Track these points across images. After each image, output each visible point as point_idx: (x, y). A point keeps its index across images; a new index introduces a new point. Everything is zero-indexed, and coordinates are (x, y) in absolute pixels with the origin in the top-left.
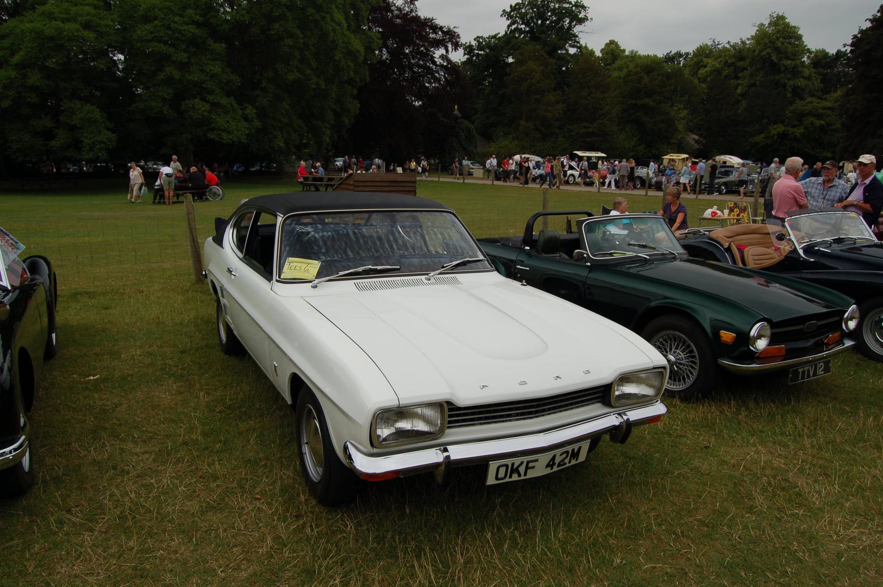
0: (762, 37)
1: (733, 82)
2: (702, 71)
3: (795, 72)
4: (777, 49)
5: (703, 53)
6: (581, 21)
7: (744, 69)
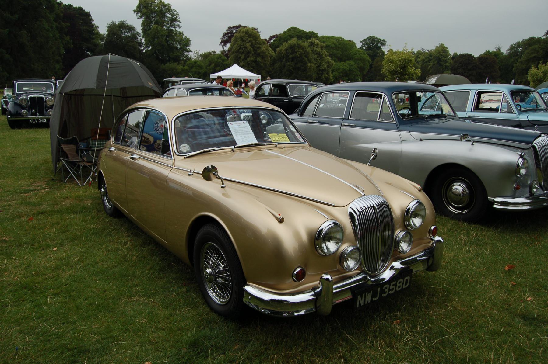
0: (437, 49)
1: (428, 63)
2: (419, 60)
3: (446, 62)
4: (441, 55)
5: (419, 53)
6: (383, 44)
7: (431, 60)
